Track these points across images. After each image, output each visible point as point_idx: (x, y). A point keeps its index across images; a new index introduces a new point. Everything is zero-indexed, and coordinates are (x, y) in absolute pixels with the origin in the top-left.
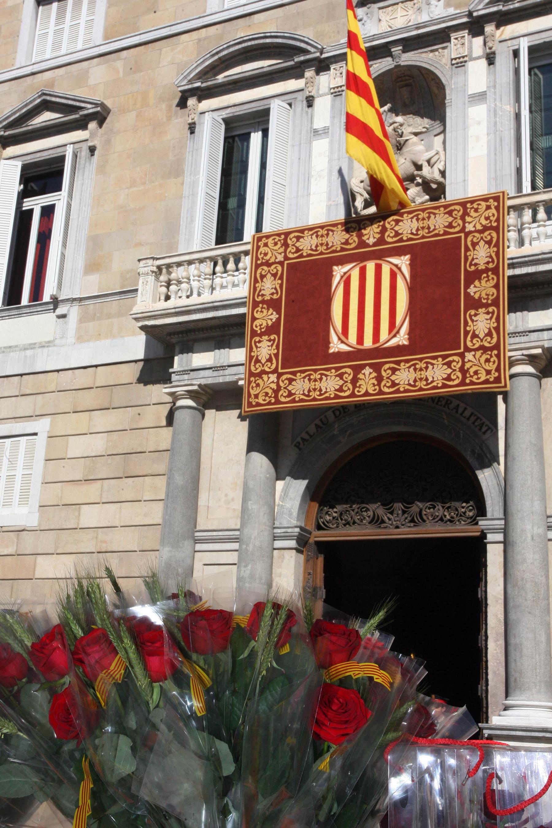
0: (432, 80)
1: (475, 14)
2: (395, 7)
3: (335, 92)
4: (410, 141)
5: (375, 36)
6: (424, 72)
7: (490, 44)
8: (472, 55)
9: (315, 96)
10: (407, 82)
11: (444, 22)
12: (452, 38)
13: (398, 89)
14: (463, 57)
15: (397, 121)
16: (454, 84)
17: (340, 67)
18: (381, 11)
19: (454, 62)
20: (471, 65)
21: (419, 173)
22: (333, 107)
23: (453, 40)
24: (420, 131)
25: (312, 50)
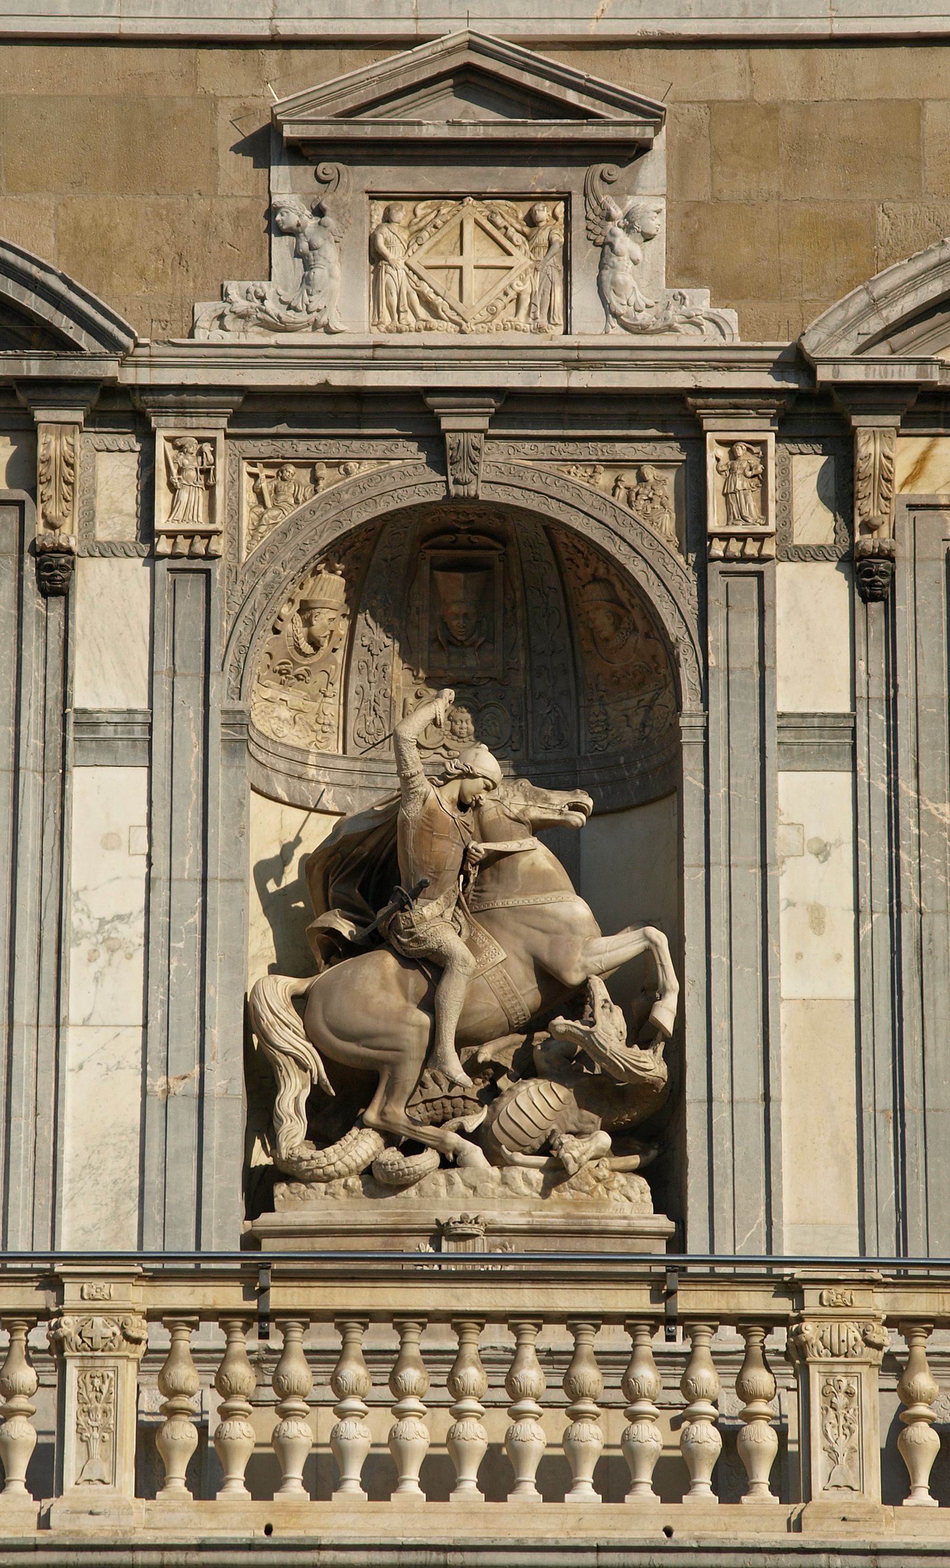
0: (595, 579)
1: (824, 374)
2: (447, 208)
4: (524, 862)
5: (380, 353)
6: (562, 538)
7: (867, 507)
9: (76, 549)
10: (476, 553)
11: (684, 366)
13: (426, 569)
14: (760, 538)
15: (477, 770)
17: (201, 440)
18: (380, 208)
20: (785, 575)
25: (84, 340)
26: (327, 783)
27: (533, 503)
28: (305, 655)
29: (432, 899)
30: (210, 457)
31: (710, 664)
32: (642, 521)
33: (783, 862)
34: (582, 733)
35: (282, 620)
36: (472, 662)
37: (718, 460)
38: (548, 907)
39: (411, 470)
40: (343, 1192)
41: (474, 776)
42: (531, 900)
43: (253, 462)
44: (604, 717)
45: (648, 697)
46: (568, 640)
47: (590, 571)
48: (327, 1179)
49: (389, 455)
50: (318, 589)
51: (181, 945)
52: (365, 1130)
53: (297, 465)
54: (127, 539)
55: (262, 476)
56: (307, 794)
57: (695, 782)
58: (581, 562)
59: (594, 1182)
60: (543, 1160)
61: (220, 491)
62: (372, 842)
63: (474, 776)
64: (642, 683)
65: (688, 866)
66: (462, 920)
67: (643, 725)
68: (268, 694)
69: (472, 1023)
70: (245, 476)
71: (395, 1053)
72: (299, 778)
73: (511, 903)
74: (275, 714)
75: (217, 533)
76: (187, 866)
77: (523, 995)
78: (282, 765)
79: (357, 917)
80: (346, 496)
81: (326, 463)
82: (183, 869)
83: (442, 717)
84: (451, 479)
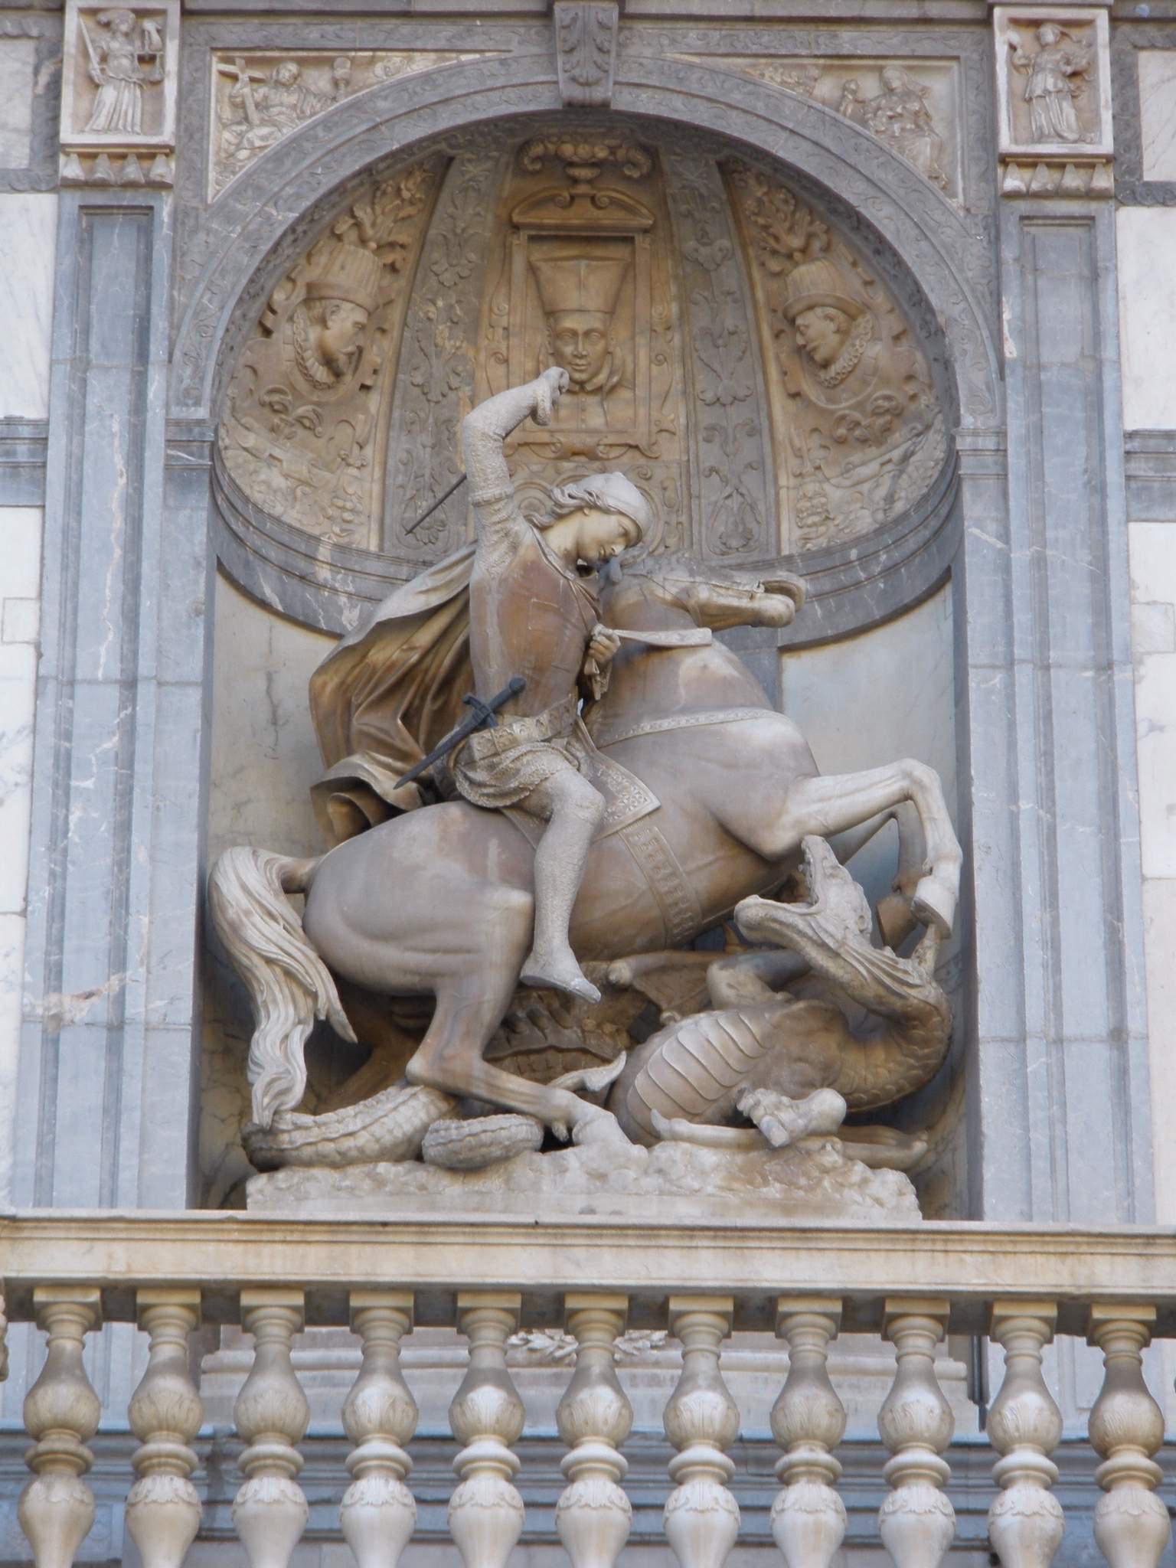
3: (102, 185)
4: (688, 666)
8: (1136, 168)
12: (997, 12)
14: (1088, 163)
16: (1021, 334)
19: (1013, 181)
21: (788, 913)
22: (76, 288)
23: (1003, 38)
24: (744, 603)
26: (350, 595)
27: (702, 116)
28: (315, 385)
29: (525, 715)
30: (156, 37)
31: (1007, 355)
32: (885, 145)
33: (1141, 662)
34: (784, 527)
35: (274, 312)
36: (596, 419)
37: (1013, 48)
38: (733, 728)
39: (495, 67)
40: (367, 1184)
41: (606, 511)
42: (702, 718)
43: (227, 53)
44: (823, 500)
45: (896, 454)
46: (760, 377)
47: (796, 242)
48: (341, 1162)
49: (459, 44)
50: (336, 267)
51: (89, 784)
52: (409, 1091)
53: (301, 62)
54: (13, 165)
55: (244, 77)
56: (315, 605)
57: (985, 537)
58: (779, 229)
59: (816, 1173)
60: (729, 1133)
61: (170, 88)
62: (425, 637)
63: (606, 511)
64: (887, 430)
65: (975, 667)
66: (581, 754)
67: (890, 499)
68: (251, 440)
69: (598, 914)
70: (215, 77)
71: (467, 956)
72: (302, 578)
73: (666, 724)
74: (262, 477)
75: (169, 151)
76: (102, 660)
77: (689, 873)
78: (273, 553)
79: (398, 765)
80: (382, 104)
81: (353, 60)
82: (96, 665)
83: (546, 405)
84: (561, 77)
